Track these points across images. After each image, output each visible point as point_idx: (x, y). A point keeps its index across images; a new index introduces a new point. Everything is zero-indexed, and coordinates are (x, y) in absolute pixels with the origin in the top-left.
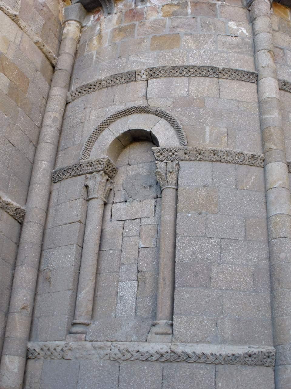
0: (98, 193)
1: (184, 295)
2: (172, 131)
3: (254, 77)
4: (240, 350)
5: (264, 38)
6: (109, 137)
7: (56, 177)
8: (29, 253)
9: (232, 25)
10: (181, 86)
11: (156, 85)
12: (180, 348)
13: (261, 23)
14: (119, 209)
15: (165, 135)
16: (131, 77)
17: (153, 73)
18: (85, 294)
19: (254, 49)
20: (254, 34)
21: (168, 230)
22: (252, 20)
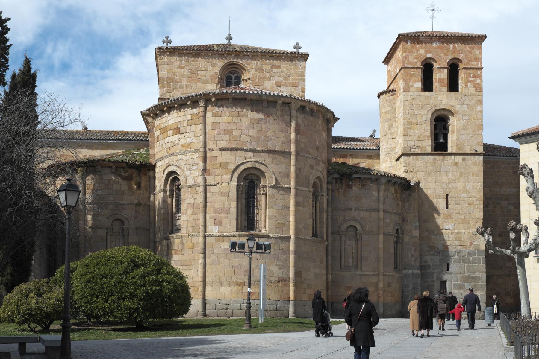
0: (344, 239)
1: (363, 263)
2: (360, 227)
3: (378, 211)
4: (373, 273)
5: (382, 198)
6: (345, 226)
7: (332, 234)
8: (330, 253)
9: (374, 193)
10: (363, 214)
11: (356, 212)
12: (363, 273)
13: (381, 193)
14: (348, 242)
15: (359, 228)
16: (351, 209)
17: (355, 210)
18: (343, 262)
19: (378, 200)
20: (379, 196)
21: (359, 249)
22: (379, 191)
